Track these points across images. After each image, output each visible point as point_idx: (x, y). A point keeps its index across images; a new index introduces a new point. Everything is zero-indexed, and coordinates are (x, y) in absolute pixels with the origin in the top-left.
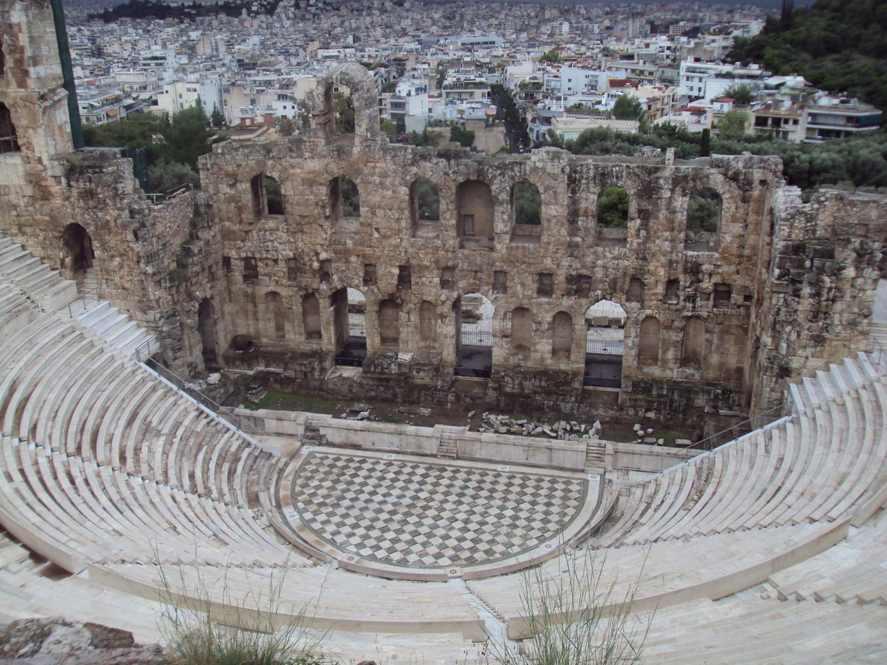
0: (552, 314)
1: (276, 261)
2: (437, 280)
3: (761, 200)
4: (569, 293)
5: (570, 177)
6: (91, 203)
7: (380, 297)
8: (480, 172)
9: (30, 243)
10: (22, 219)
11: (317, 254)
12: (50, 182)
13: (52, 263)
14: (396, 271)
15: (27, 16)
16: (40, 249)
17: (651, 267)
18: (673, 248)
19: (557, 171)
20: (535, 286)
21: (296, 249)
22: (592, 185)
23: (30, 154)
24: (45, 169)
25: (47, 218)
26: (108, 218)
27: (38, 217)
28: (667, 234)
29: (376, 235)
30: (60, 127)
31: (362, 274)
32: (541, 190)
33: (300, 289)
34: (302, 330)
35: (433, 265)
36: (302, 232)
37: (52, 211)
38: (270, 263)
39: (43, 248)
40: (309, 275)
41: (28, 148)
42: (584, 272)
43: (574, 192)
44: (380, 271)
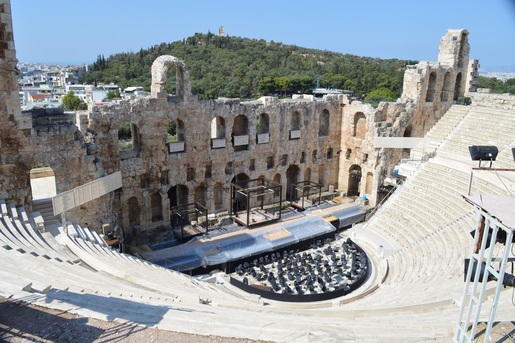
0: (274, 176)
1: (134, 177)
2: (224, 170)
3: (341, 112)
4: (280, 164)
5: (281, 109)
7: (196, 185)
8: (245, 110)
11: (161, 168)
14: (204, 169)
16: (5, 192)
17: (309, 146)
18: (315, 136)
19: (275, 107)
20: (266, 164)
21: (148, 166)
22: (288, 112)
24: (16, 123)
25: (13, 165)
26: (74, 156)
28: (314, 130)
29: (195, 150)
31: (186, 175)
32: (270, 117)
33: (150, 191)
34: (151, 217)
35: (224, 162)
36: (152, 156)
38: (131, 179)
39: (8, 191)
40: (156, 182)
42: (285, 153)
43: (282, 116)
44: (197, 171)
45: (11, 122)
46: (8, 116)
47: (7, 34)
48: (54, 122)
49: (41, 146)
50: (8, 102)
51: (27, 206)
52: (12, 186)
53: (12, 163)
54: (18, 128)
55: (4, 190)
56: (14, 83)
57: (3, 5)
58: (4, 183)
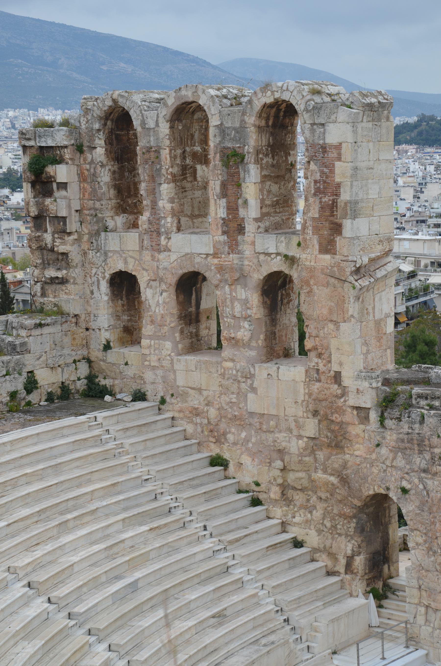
6: (419, 461)
9: (297, 519)
10: (291, 477)
12: (350, 416)
13: (329, 563)
15: (355, 132)
16: (313, 533)
23: (321, 367)
27: (320, 475)
30: (378, 323)
37: (345, 466)
39: (319, 532)
41: (320, 355)
45: (336, 386)
46: (332, 373)
47: (343, 204)
48: (423, 403)
49: (384, 451)
50: (334, 343)
51: (348, 577)
52: (328, 524)
53: (332, 475)
54: (347, 403)
55: (312, 527)
56: (346, 305)
57: (341, 144)
58: (314, 512)
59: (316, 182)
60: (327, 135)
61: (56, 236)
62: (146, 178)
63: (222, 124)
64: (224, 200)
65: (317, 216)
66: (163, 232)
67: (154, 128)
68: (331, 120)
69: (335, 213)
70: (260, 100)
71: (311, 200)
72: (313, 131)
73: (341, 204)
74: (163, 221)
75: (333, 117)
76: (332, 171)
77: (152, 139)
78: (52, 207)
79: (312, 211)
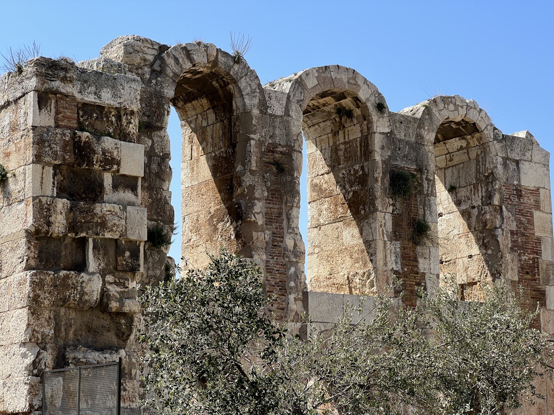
47: (545, 267)
57: (538, 189)
59: (512, 233)
60: (522, 176)
61: (110, 278)
62: (266, 194)
63: (391, 132)
64: (398, 244)
65: (516, 279)
66: (291, 288)
67: (281, 117)
68: (526, 158)
69: (537, 276)
70: (442, 112)
71: (508, 257)
72: (505, 165)
73: (543, 266)
74: (293, 270)
75: (528, 154)
76: (531, 222)
77: (277, 132)
78: (112, 220)
79: (510, 272)
